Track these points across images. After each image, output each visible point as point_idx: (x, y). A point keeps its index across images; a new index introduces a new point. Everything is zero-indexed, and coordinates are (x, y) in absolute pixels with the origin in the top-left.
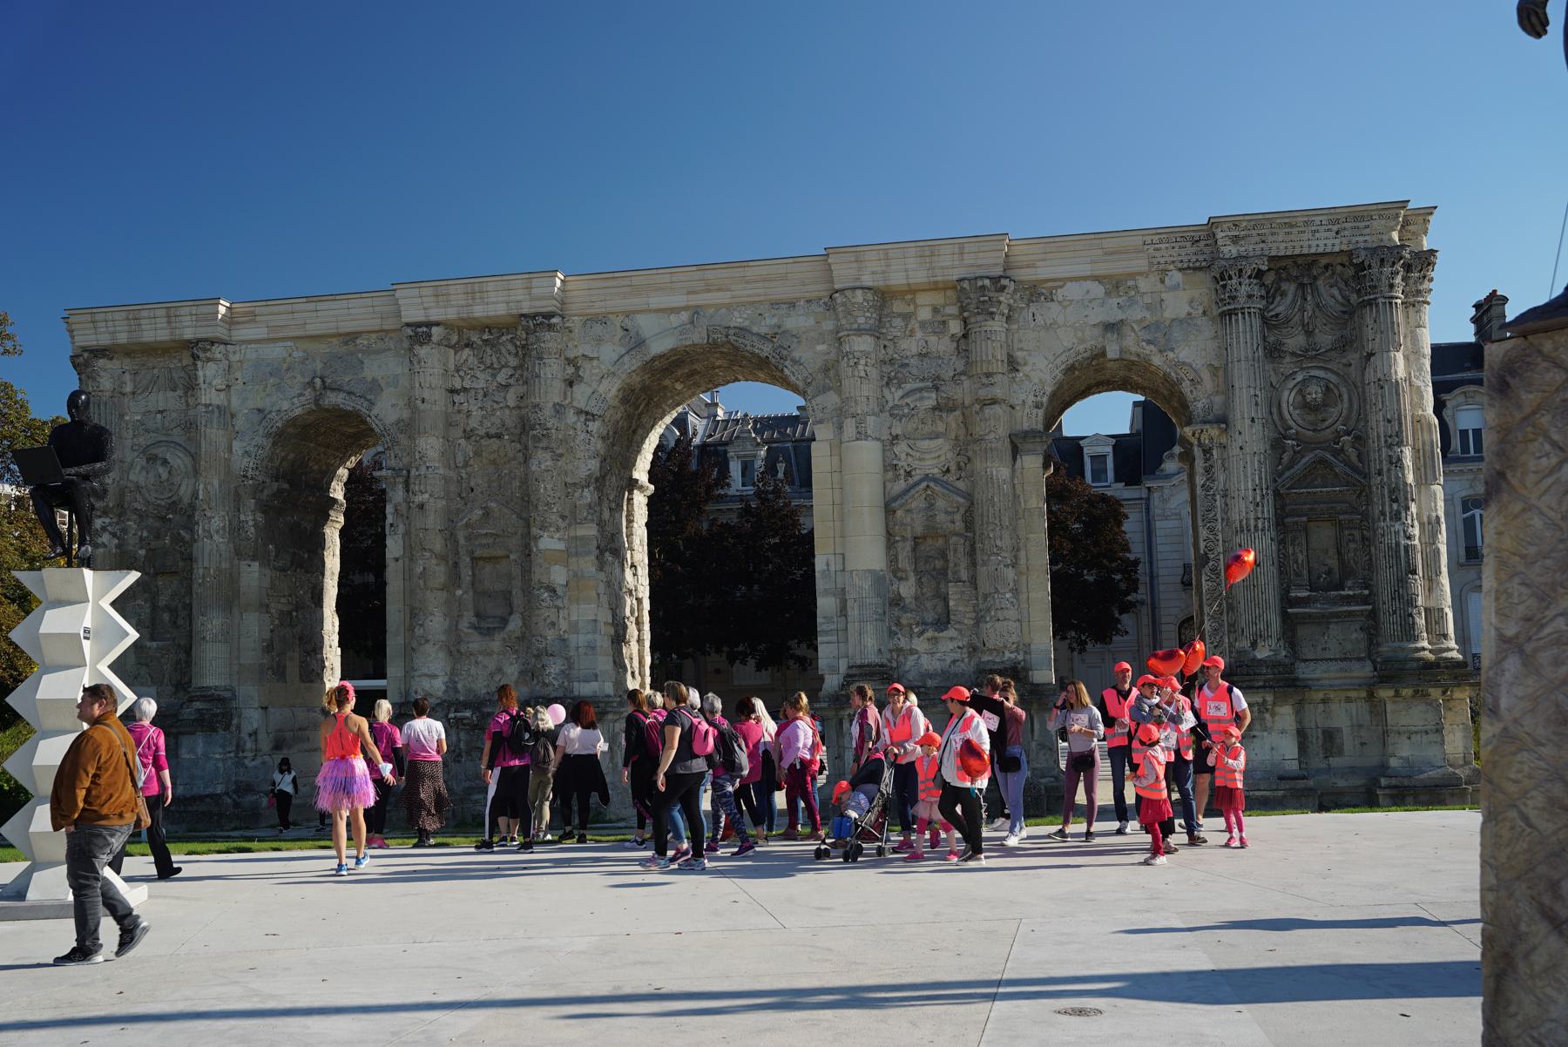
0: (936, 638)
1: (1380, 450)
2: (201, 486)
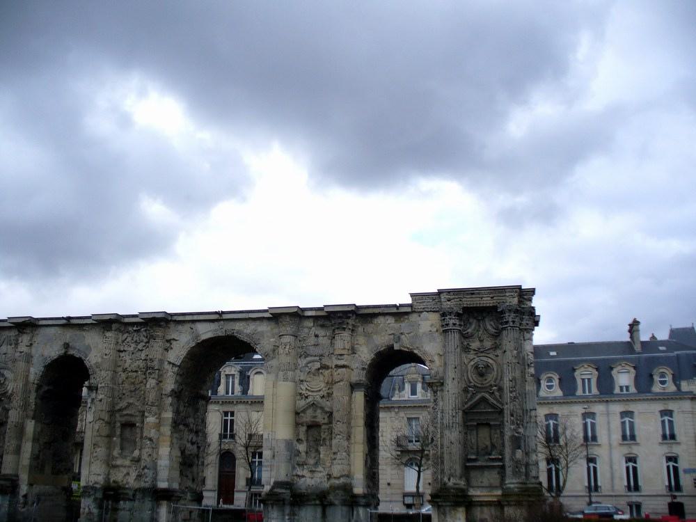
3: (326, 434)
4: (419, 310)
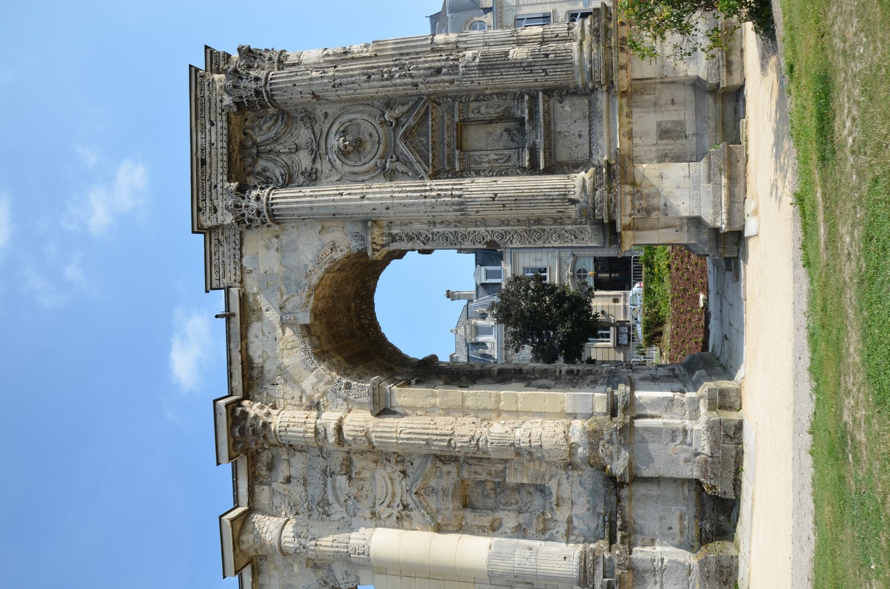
0: (558, 499)
1: (395, 85)
3: (479, 470)
4: (238, 273)
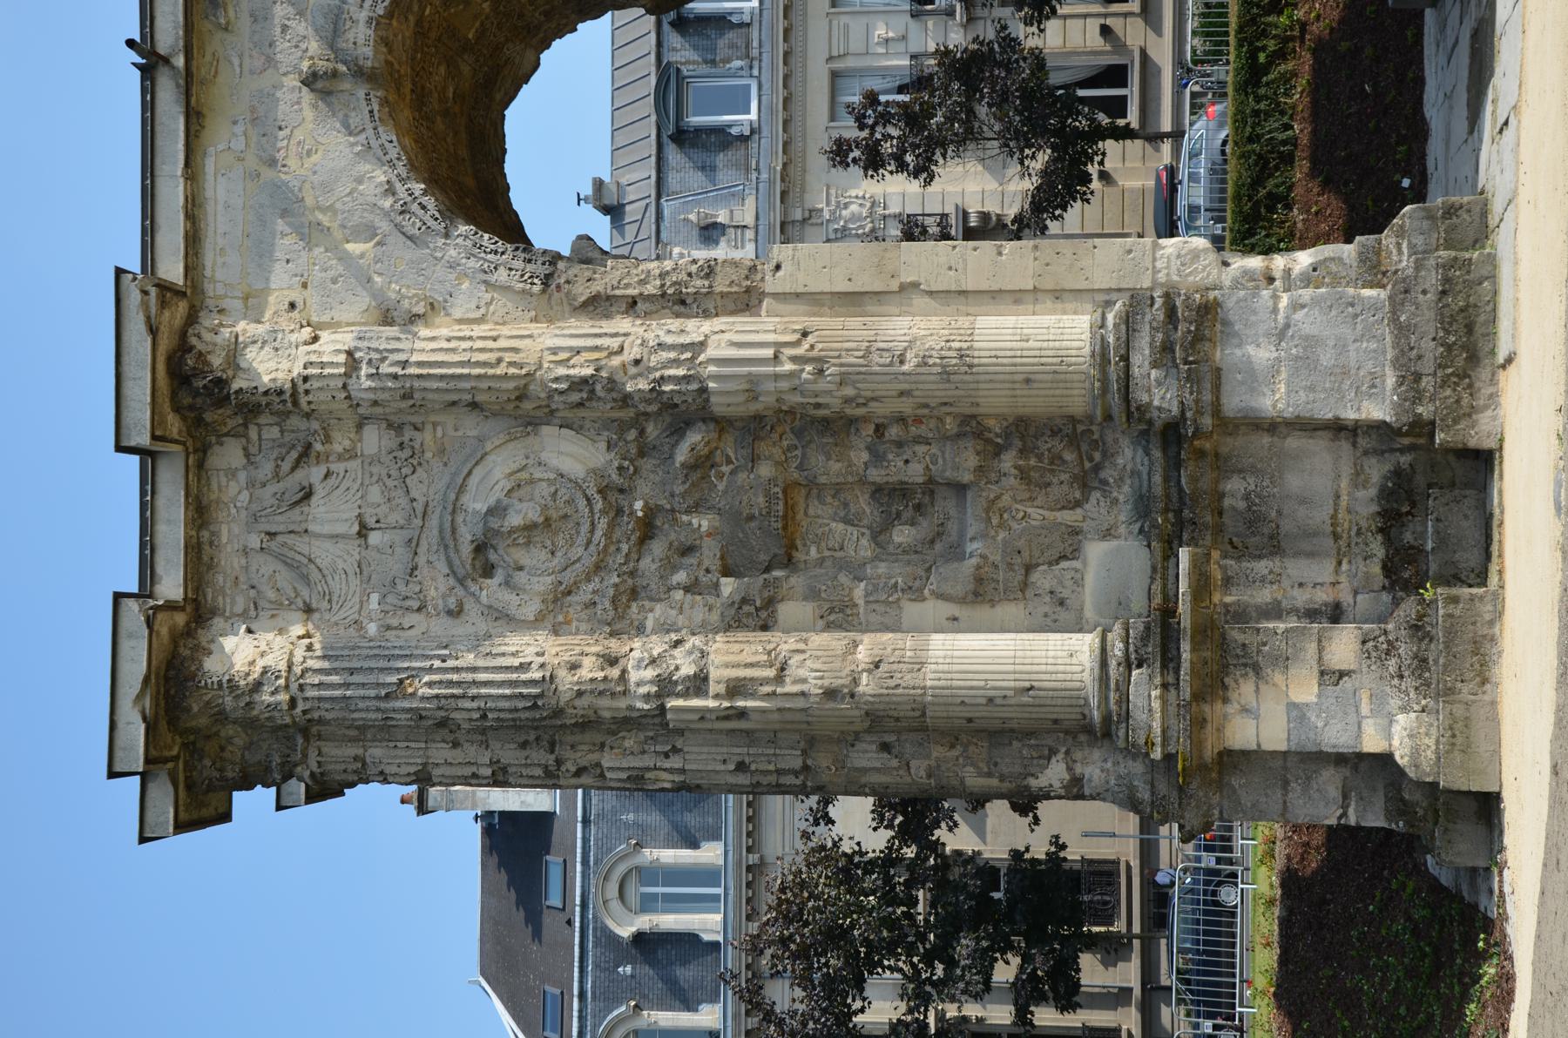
2: (562, 371)
